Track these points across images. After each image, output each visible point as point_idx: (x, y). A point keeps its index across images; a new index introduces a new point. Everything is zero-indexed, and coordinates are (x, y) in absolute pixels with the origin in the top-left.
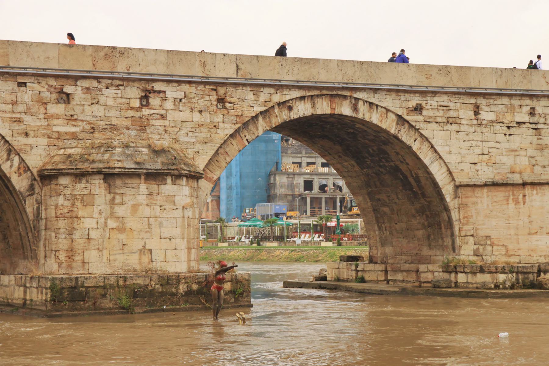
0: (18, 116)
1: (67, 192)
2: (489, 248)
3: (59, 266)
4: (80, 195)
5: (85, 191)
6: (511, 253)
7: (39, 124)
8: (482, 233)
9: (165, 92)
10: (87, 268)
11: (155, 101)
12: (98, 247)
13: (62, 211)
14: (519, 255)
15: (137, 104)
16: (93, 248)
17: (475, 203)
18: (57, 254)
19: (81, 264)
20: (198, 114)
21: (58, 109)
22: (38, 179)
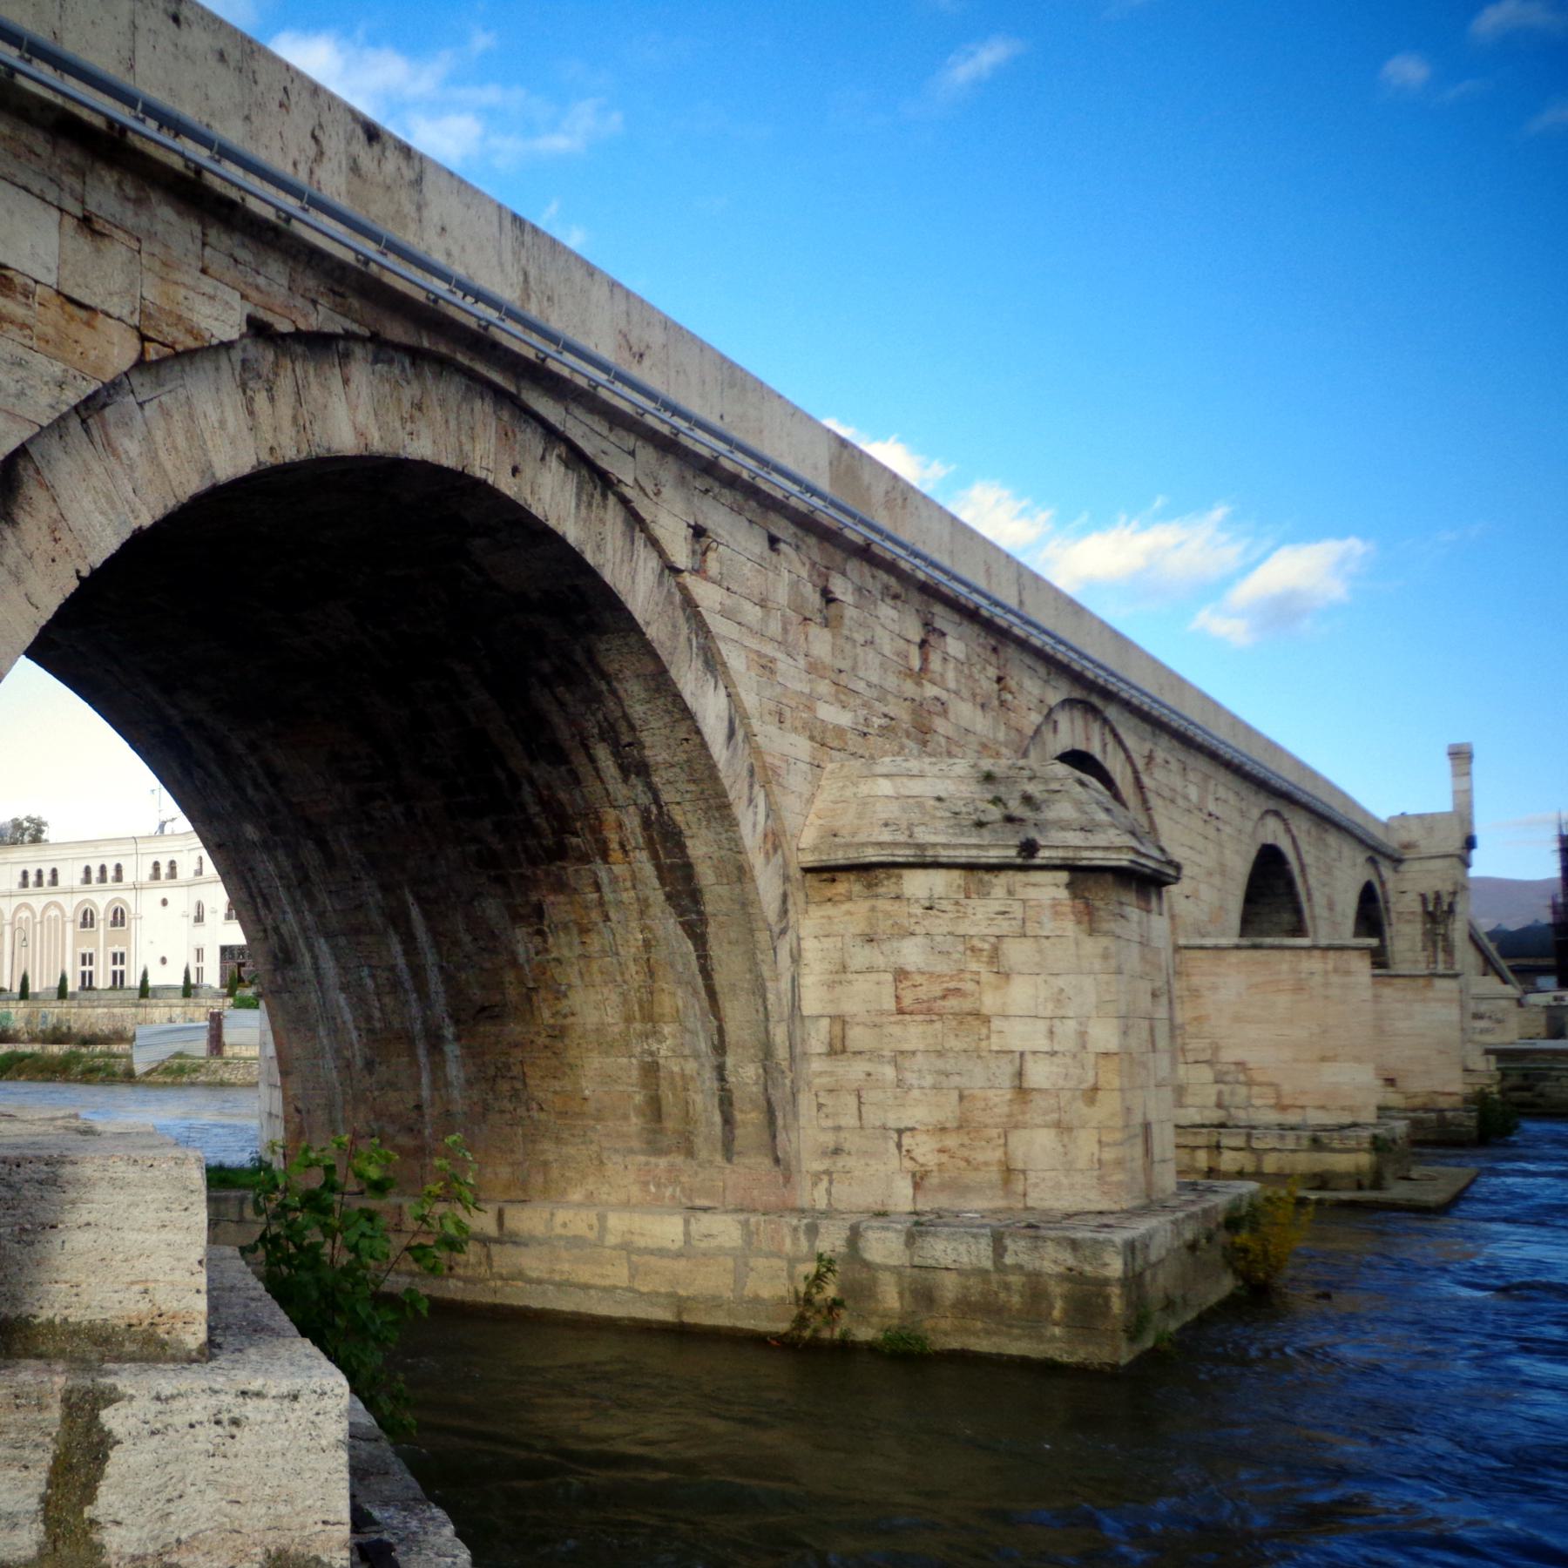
0: (769, 649)
1: (939, 925)
2: (1242, 1091)
3: (916, 1186)
4: (983, 938)
5: (1005, 924)
6: (1286, 1101)
7: (799, 687)
8: (1228, 1056)
9: (943, 634)
10: (1020, 1188)
11: (935, 663)
12: (1055, 1116)
13: (922, 993)
14: (1303, 1107)
15: (916, 663)
16: (1038, 1120)
17: (1214, 988)
18: (907, 1140)
19: (994, 1175)
20: (979, 712)
21: (821, 643)
22: (799, 874)
